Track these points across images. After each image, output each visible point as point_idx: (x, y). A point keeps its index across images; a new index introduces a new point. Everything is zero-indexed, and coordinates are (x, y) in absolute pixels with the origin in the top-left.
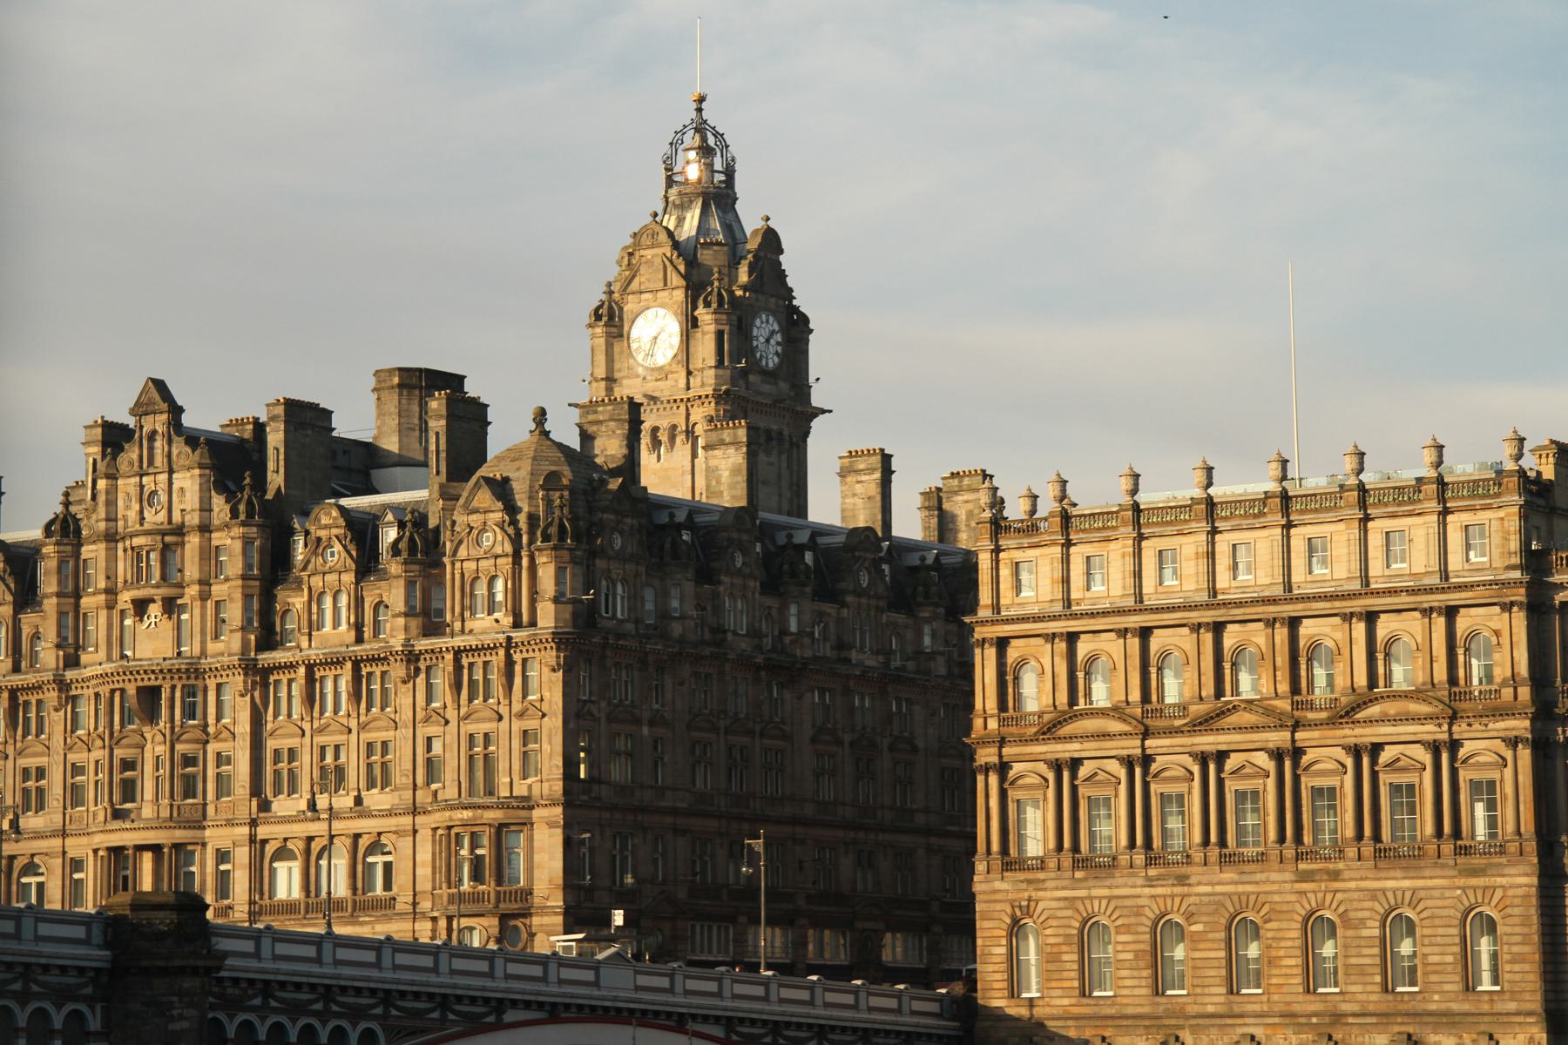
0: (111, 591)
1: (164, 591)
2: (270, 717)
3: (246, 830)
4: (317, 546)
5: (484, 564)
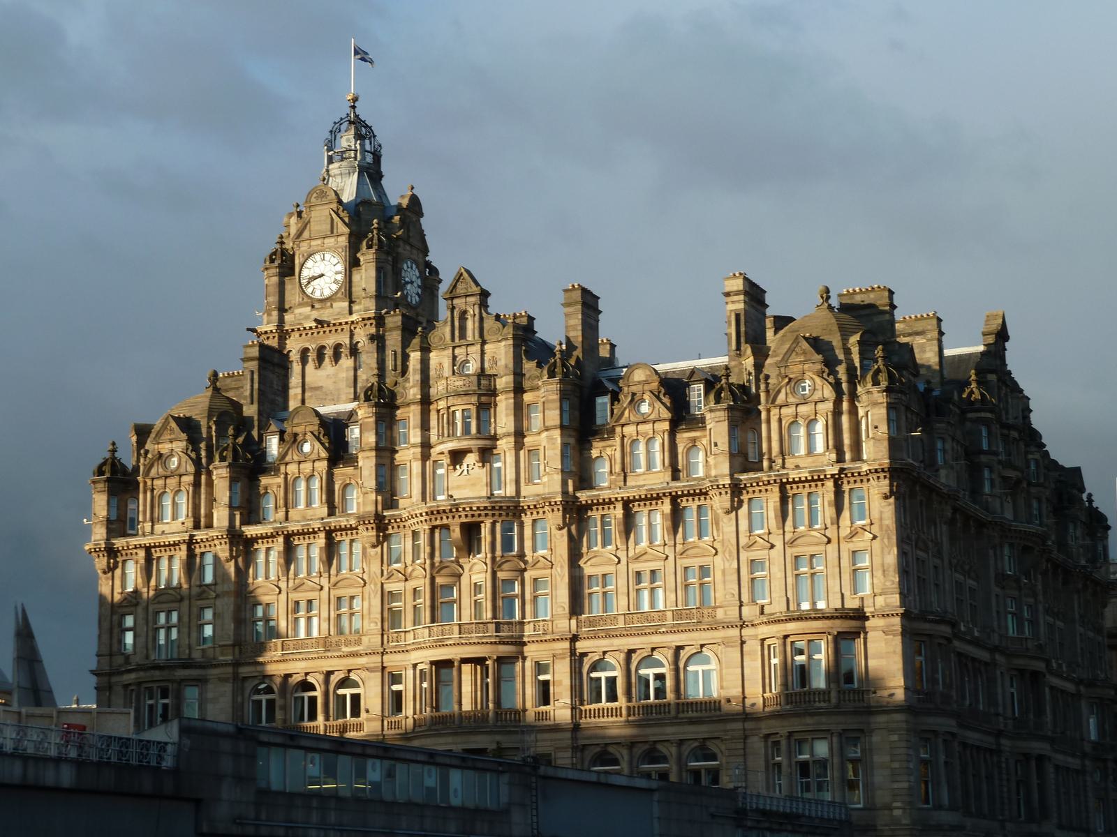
0: (426, 446)
1: (481, 443)
2: (584, 550)
3: (566, 645)
4: (635, 401)
5: (803, 409)
